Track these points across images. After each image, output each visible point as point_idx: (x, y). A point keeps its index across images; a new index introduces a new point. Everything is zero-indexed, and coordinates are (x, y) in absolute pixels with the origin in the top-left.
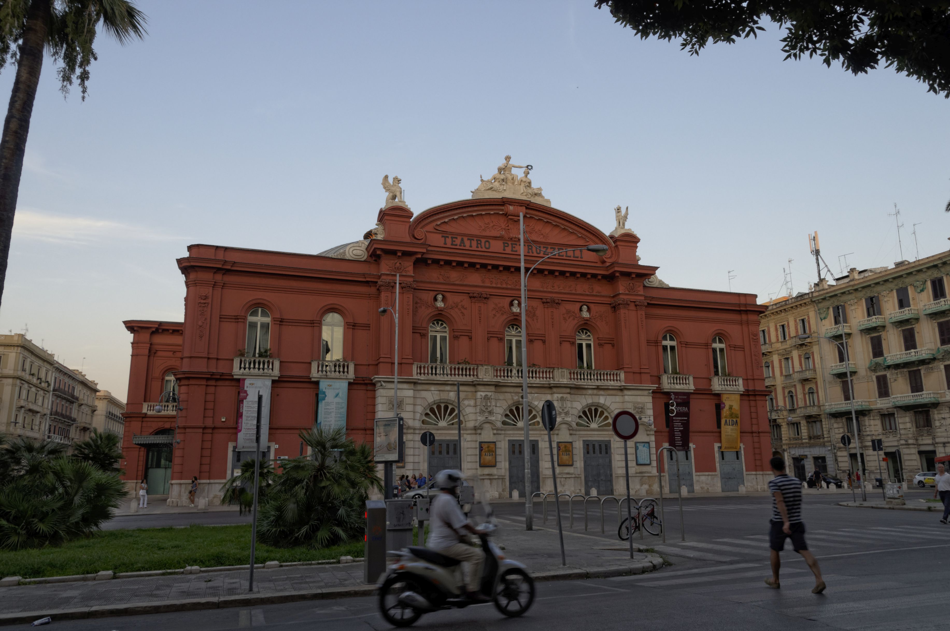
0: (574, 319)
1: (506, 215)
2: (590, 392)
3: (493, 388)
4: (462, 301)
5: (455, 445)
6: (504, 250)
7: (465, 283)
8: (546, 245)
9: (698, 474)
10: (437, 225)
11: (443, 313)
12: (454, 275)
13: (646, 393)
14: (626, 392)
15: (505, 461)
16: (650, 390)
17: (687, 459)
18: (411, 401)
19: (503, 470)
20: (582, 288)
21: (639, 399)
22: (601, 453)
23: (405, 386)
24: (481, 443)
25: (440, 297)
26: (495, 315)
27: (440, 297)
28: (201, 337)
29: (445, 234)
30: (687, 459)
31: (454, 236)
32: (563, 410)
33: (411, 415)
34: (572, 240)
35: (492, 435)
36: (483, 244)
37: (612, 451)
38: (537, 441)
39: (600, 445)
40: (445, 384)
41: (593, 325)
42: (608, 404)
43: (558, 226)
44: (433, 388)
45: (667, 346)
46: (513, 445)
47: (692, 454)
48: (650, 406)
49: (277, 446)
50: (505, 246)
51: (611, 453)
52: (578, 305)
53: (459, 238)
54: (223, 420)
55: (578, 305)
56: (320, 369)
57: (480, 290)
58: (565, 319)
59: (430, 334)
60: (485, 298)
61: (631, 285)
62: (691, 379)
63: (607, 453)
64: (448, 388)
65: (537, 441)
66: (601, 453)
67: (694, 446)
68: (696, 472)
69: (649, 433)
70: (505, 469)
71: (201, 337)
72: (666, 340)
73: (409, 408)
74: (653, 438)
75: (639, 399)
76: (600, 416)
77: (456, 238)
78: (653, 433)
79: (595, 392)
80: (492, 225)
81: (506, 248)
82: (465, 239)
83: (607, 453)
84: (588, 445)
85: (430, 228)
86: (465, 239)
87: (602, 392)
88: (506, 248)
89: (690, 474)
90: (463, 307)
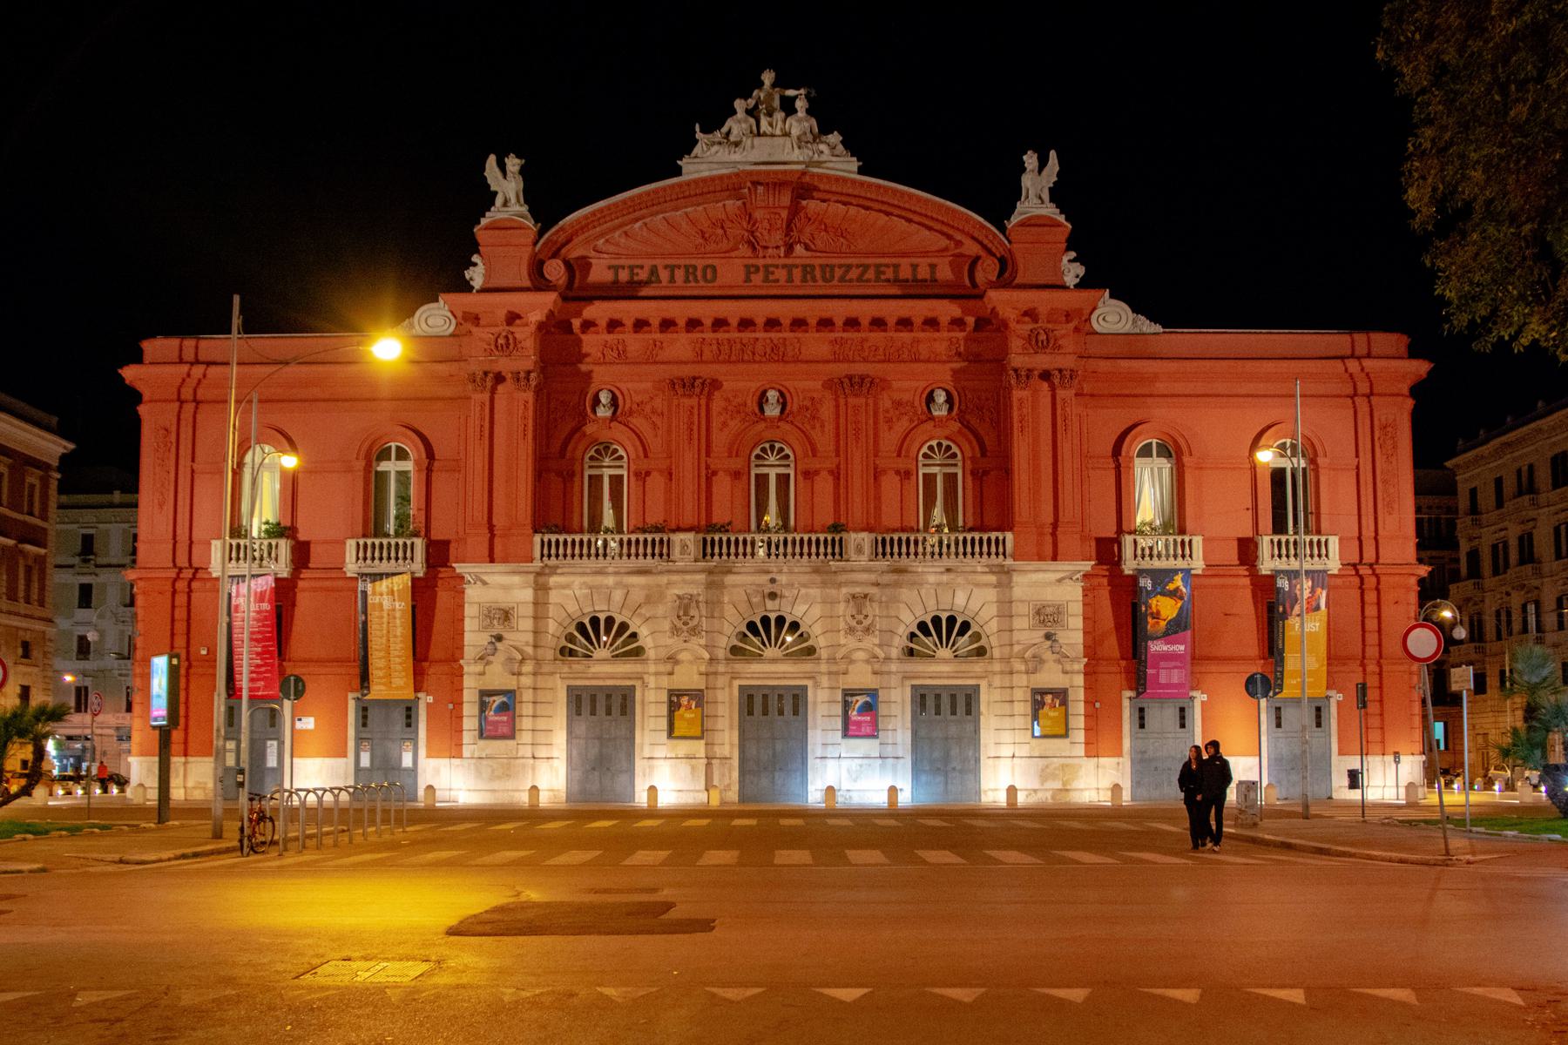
3: (701, 577)
5: (624, 697)
6: (748, 280)
15: (731, 728)
18: (530, 610)
19: (727, 747)
22: (954, 713)
23: (516, 579)
24: (671, 693)
26: (725, 424)
28: (161, 506)
32: (859, 623)
33: (530, 637)
35: (696, 677)
36: (699, 274)
37: (983, 708)
38: (805, 688)
39: (953, 697)
40: (601, 572)
42: (974, 605)
44: (578, 580)
46: (750, 697)
48: (1077, 608)
50: (748, 273)
51: (979, 713)
54: (204, 652)
56: (361, 555)
58: (889, 421)
59: (587, 473)
63: (969, 712)
64: (610, 580)
65: (805, 688)
66: (954, 713)
67: (1205, 697)
69: (1068, 668)
70: (732, 745)
71: (161, 506)
73: (527, 624)
74: (1079, 680)
76: (962, 632)
77: (642, 267)
79: (945, 578)
81: (753, 277)
83: (969, 712)
84: (923, 696)
87: (960, 580)
88: (753, 277)
90: (654, 411)
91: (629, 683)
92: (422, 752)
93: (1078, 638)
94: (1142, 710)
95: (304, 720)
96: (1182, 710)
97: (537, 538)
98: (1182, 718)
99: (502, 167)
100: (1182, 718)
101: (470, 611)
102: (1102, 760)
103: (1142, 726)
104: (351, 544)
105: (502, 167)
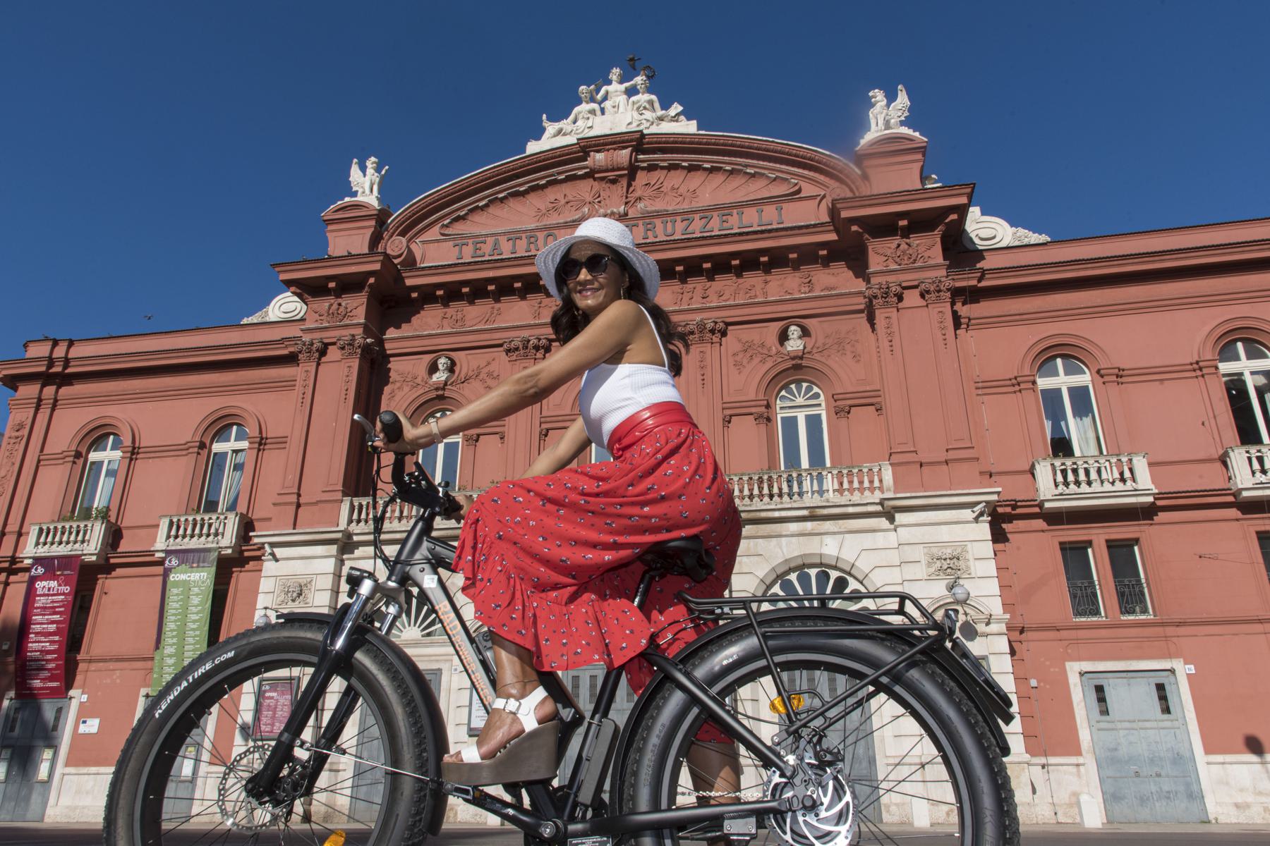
0: (763, 361)
1: (591, 175)
2: (794, 527)
4: (489, 364)
7: (495, 326)
8: (687, 215)
9: (1219, 758)
10: (443, 226)
11: (447, 394)
12: (475, 314)
13: (968, 514)
14: (900, 518)
16: (979, 503)
17: (1166, 710)
20: (780, 287)
21: (945, 534)
25: (442, 362)
27: (442, 362)
29: (460, 240)
30: (1166, 710)
31: (479, 240)
34: (757, 189)
41: (818, 366)
43: (719, 169)
45: (1058, 391)
47: (1183, 695)
49: (84, 698)
52: (776, 327)
53: (490, 240)
55: (776, 327)
57: (525, 334)
60: (537, 348)
61: (904, 246)
62: (1141, 464)
67: (1191, 669)
68: (1208, 750)
72: (1057, 374)
75: (945, 534)
78: (1002, 628)
79: (809, 525)
80: (563, 202)
82: (503, 240)
85: (434, 233)
86: (503, 240)
87: (829, 526)
89: (1183, 762)
90: (489, 374)
91: (435, 666)
92: (206, 756)
93: (993, 587)
94: (1099, 689)
95: (90, 721)
96: (1160, 688)
97: (347, 501)
98: (1163, 698)
99: (363, 169)
100: (1163, 698)
101: (265, 585)
102: (1052, 760)
103: (1105, 712)
104: (164, 524)
105: (363, 169)
